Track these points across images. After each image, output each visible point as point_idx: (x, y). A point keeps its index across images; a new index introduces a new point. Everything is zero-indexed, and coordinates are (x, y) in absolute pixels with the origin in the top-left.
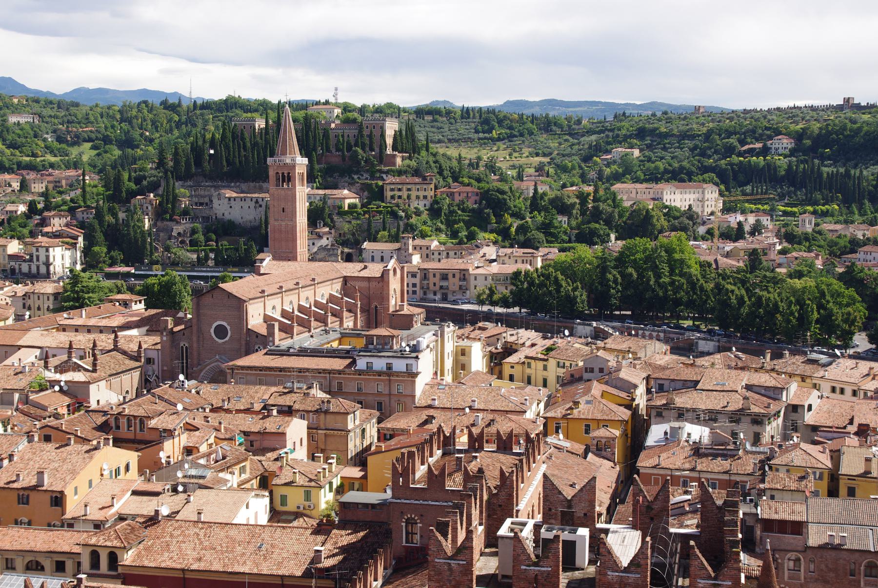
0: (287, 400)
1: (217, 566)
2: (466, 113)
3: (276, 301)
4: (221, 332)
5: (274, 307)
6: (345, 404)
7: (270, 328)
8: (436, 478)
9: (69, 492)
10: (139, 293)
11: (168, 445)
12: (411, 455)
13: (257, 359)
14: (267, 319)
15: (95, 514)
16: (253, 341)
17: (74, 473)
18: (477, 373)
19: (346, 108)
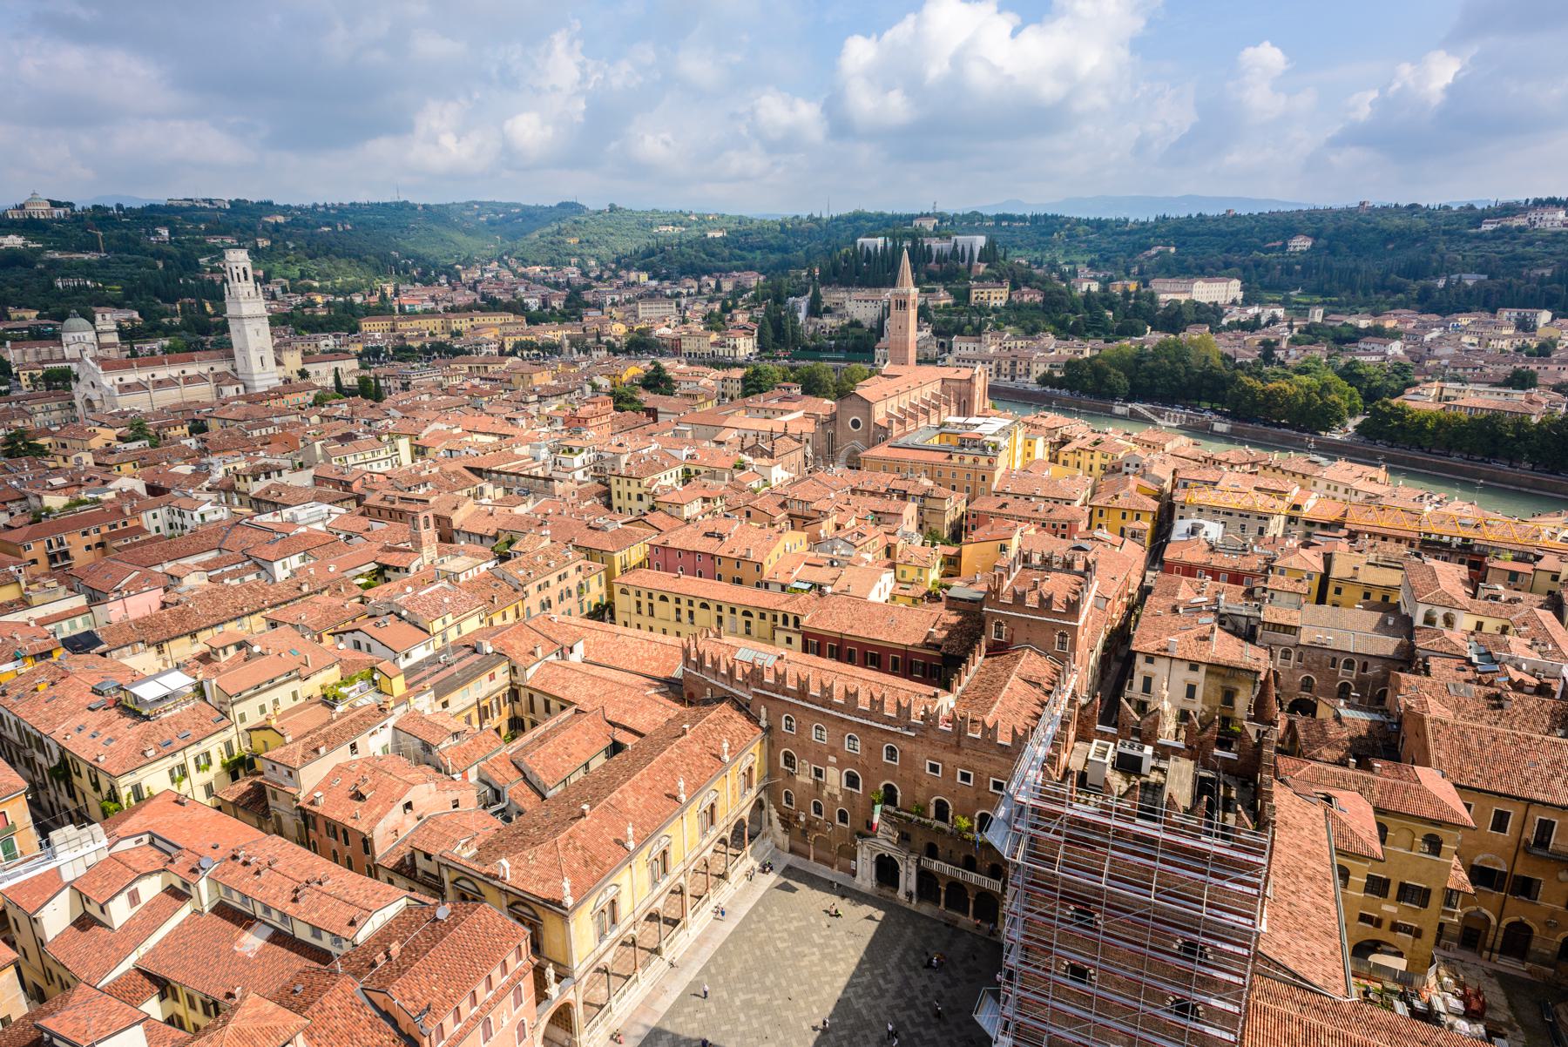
0: (900, 485)
1: (863, 634)
2: (1035, 218)
3: (893, 401)
4: (856, 424)
5: (892, 405)
6: (944, 491)
7: (890, 422)
8: (1019, 599)
9: (765, 563)
10: (795, 381)
11: (825, 524)
12: (1001, 576)
13: (881, 451)
14: (889, 415)
15: (781, 578)
16: (880, 435)
17: (769, 550)
18: (1040, 461)
19: (942, 218)
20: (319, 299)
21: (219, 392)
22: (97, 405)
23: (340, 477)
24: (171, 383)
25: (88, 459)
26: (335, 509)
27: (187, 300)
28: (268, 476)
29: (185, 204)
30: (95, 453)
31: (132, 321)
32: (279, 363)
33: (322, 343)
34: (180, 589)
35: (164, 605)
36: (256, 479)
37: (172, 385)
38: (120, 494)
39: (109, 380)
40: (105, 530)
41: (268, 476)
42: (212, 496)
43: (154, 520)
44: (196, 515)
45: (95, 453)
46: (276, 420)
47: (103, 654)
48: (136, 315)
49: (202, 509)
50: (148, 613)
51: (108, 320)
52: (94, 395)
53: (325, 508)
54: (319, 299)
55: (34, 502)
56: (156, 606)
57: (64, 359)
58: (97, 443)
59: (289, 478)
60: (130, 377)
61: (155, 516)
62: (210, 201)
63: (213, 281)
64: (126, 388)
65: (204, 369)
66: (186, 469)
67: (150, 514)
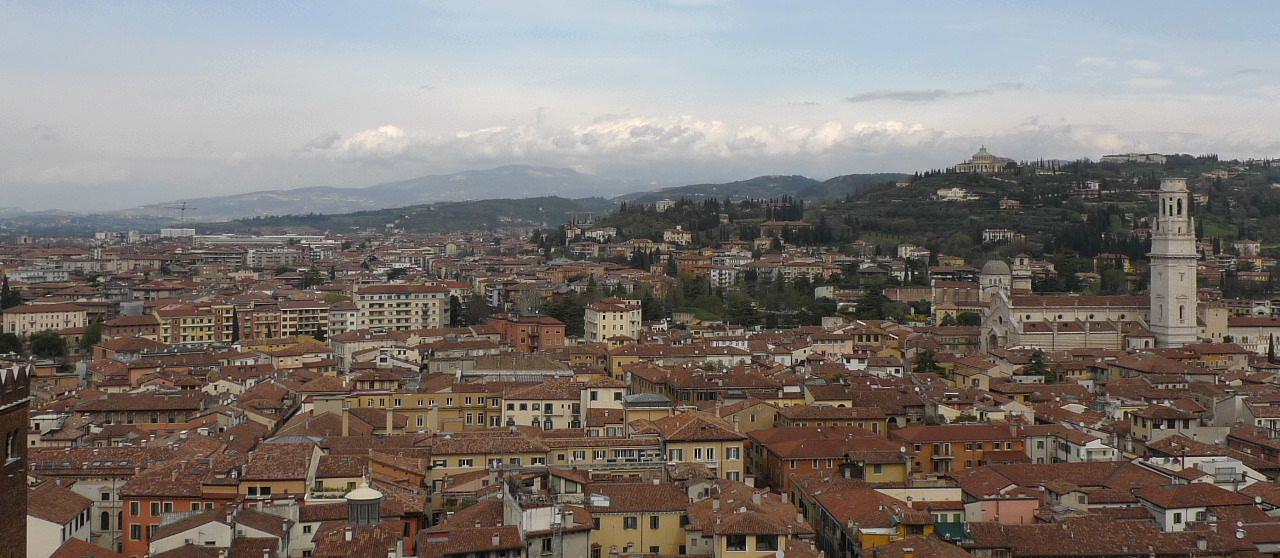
20: (1258, 263)
21: (1125, 344)
22: (1000, 340)
23: (1264, 442)
24: (1076, 326)
25: (984, 385)
26: (1251, 472)
27: (1105, 255)
28: (1171, 426)
29: (1121, 161)
30: (991, 380)
31: (1047, 272)
32: (1200, 323)
33: (1256, 310)
34: (1056, 508)
35: (1037, 519)
36: (1156, 426)
37: (1078, 328)
38: (1009, 417)
39: (1016, 318)
40: (988, 448)
41: (1171, 426)
42: (1104, 435)
43: (1036, 450)
44: (1083, 450)
45: (991, 380)
46: (1188, 378)
47: (969, 549)
48: (1051, 267)
49: (1091, 445)
50: (1018, 522)
51: (1024, 267)
52: (999, 331)
53: (1240, 467)
54: (1258, 263)
55: (929, 411)
56: (1028, 519)
57: (977, 304)
58: (994, 372)
59: (1193, 431)
60: (1037, 317)
61: (1040, 445)
62: (1148, 157)
63: (1136, 239)
64: (1032, 327)
65: (1114, 316)
66: (1078, 408)
67: (1036, 440)
